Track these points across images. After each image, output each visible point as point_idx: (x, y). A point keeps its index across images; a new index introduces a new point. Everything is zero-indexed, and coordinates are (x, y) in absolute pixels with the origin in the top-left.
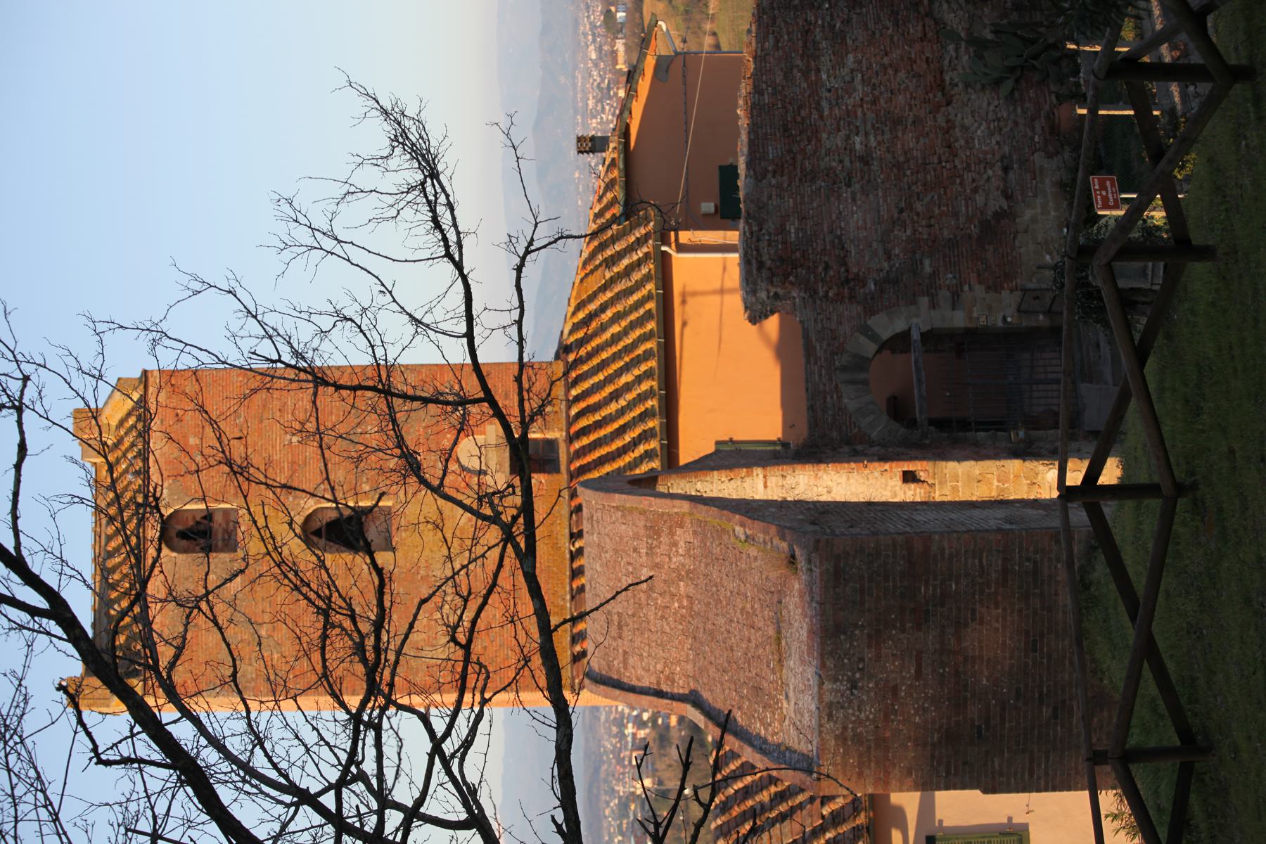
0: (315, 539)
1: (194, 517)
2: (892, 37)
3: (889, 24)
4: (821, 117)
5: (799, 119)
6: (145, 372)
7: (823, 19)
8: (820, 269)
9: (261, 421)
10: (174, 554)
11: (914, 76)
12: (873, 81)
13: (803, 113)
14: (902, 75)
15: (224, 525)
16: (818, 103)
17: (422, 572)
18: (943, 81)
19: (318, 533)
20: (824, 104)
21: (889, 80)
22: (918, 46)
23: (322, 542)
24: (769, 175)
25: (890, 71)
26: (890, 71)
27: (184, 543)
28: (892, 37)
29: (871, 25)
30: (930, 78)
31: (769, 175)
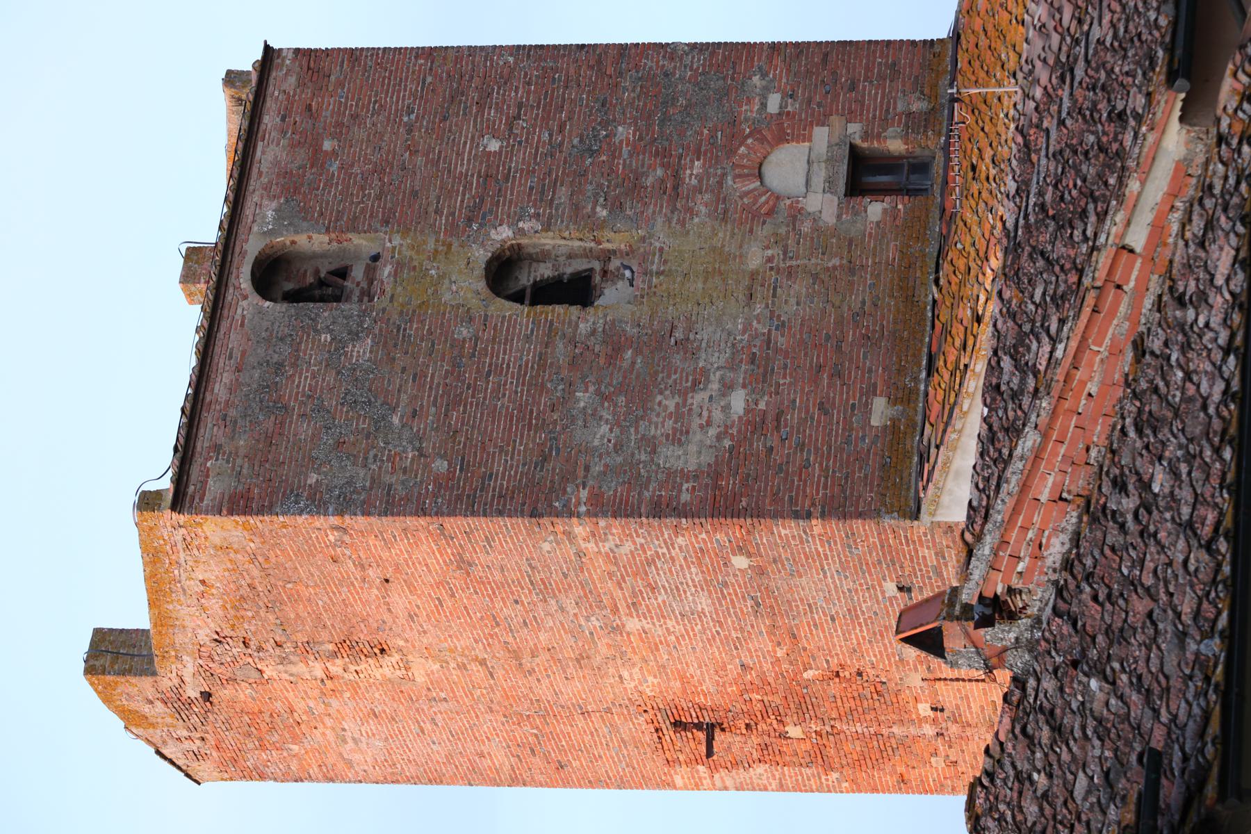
1: (317, 271)
6: (267, 49)
9: (445, 119)
10: (268, 303)
15: (364, 285)
17: (678, 334)
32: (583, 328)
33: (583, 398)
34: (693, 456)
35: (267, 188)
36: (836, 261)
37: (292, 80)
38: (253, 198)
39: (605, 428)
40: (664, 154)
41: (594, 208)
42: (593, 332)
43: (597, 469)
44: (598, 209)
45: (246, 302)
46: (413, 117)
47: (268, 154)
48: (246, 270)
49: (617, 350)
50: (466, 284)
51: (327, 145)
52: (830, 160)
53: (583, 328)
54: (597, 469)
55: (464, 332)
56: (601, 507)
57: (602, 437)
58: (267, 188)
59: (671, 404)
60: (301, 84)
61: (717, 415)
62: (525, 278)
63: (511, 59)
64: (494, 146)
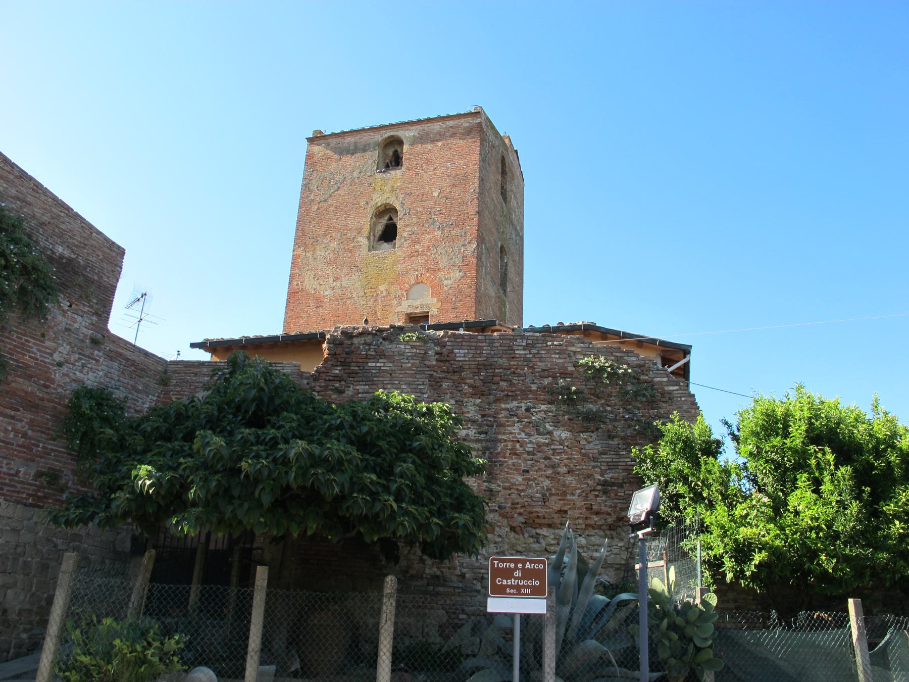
0: (387, 218)
2: (590, 476)
3: (608, 476)
4: (498, 400)
5: (496, 379)
7: (611, 412)
8: (337, 385)
11: (544, 495)
12: (539, 455)
13: (504, 384)
14: (547, 483)
16: (514, 398)
18: (541, 526)
19: (391, 219)
20: (515, 404)
21: (540, 470)
22: (580, 502)
23: (384, 221)
24: (437, 349)
25: (550, 472)
26: (550, 472)
27: (391, 153)
28: (590, 476)
29: (605, 458)
30: (542, 511)
31: (437, 349)
33: (334, 245)
34: (309, 283)
35: (423, 130)
36: (379, 314)
37: (467, 125)
38: (419, 127)
42: (358, 242)
45: (379, 137)
47: (437, 127)
48: (392, 134)
49: (350, 251)
50: (379, 200)
51: (440, 144)
52: (422, 306)
53: (360, 239)
55: (363, 203)
56: (295, 258)
58: (423, 130)
59: (329, 272)
60: (465, 128)
61: (323, 287)
62: (395, 220)
64: (435, 194)
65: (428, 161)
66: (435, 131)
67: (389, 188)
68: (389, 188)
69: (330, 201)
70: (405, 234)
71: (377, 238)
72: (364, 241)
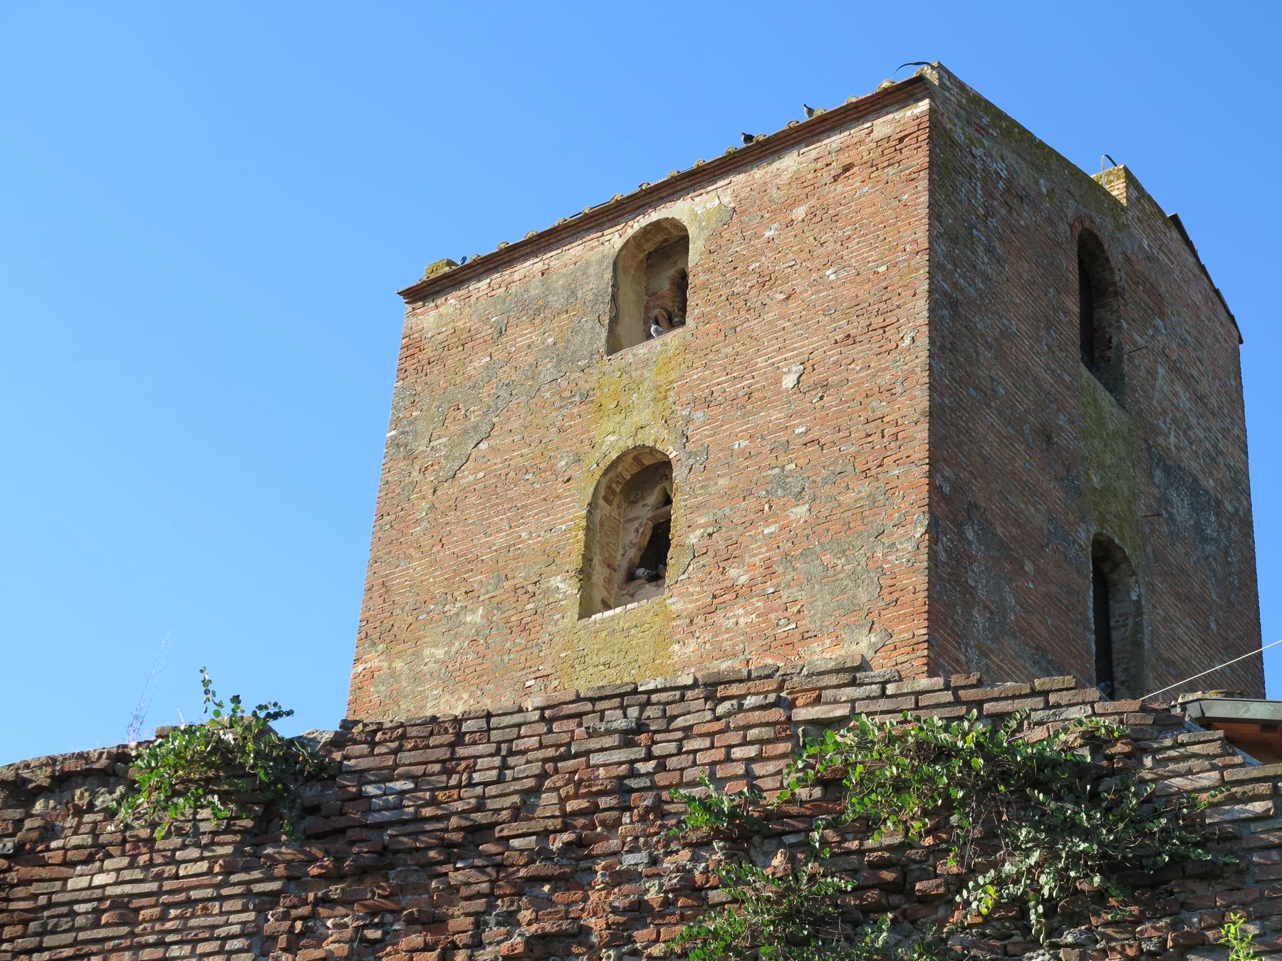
32: (556, 581)
39: (440, 653)
40: (769, 568)
41: (699, 527)
43: (398, 664)
44: (698, 532)
46: (832, 277)
48: (654, 216)
49: (525, 628)
50: (613, 439)
51: (800, 212)
53: (556, 581)
54: (398, 664)
57: (432, 655)
63: (908, 341)
64: (789, 382)
65: (766, 281)
66: (786, 177)
67: (644, 396)
68: (644, 396)
69: (466, 478)
70: (693, 538)
71: (620, 576)
72: (565, 587)
